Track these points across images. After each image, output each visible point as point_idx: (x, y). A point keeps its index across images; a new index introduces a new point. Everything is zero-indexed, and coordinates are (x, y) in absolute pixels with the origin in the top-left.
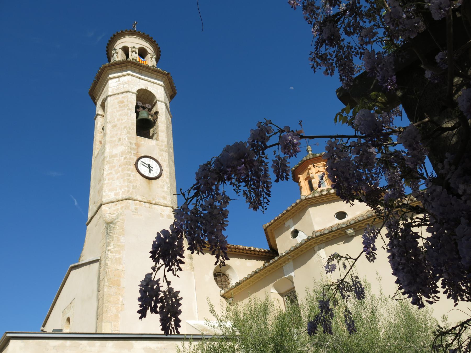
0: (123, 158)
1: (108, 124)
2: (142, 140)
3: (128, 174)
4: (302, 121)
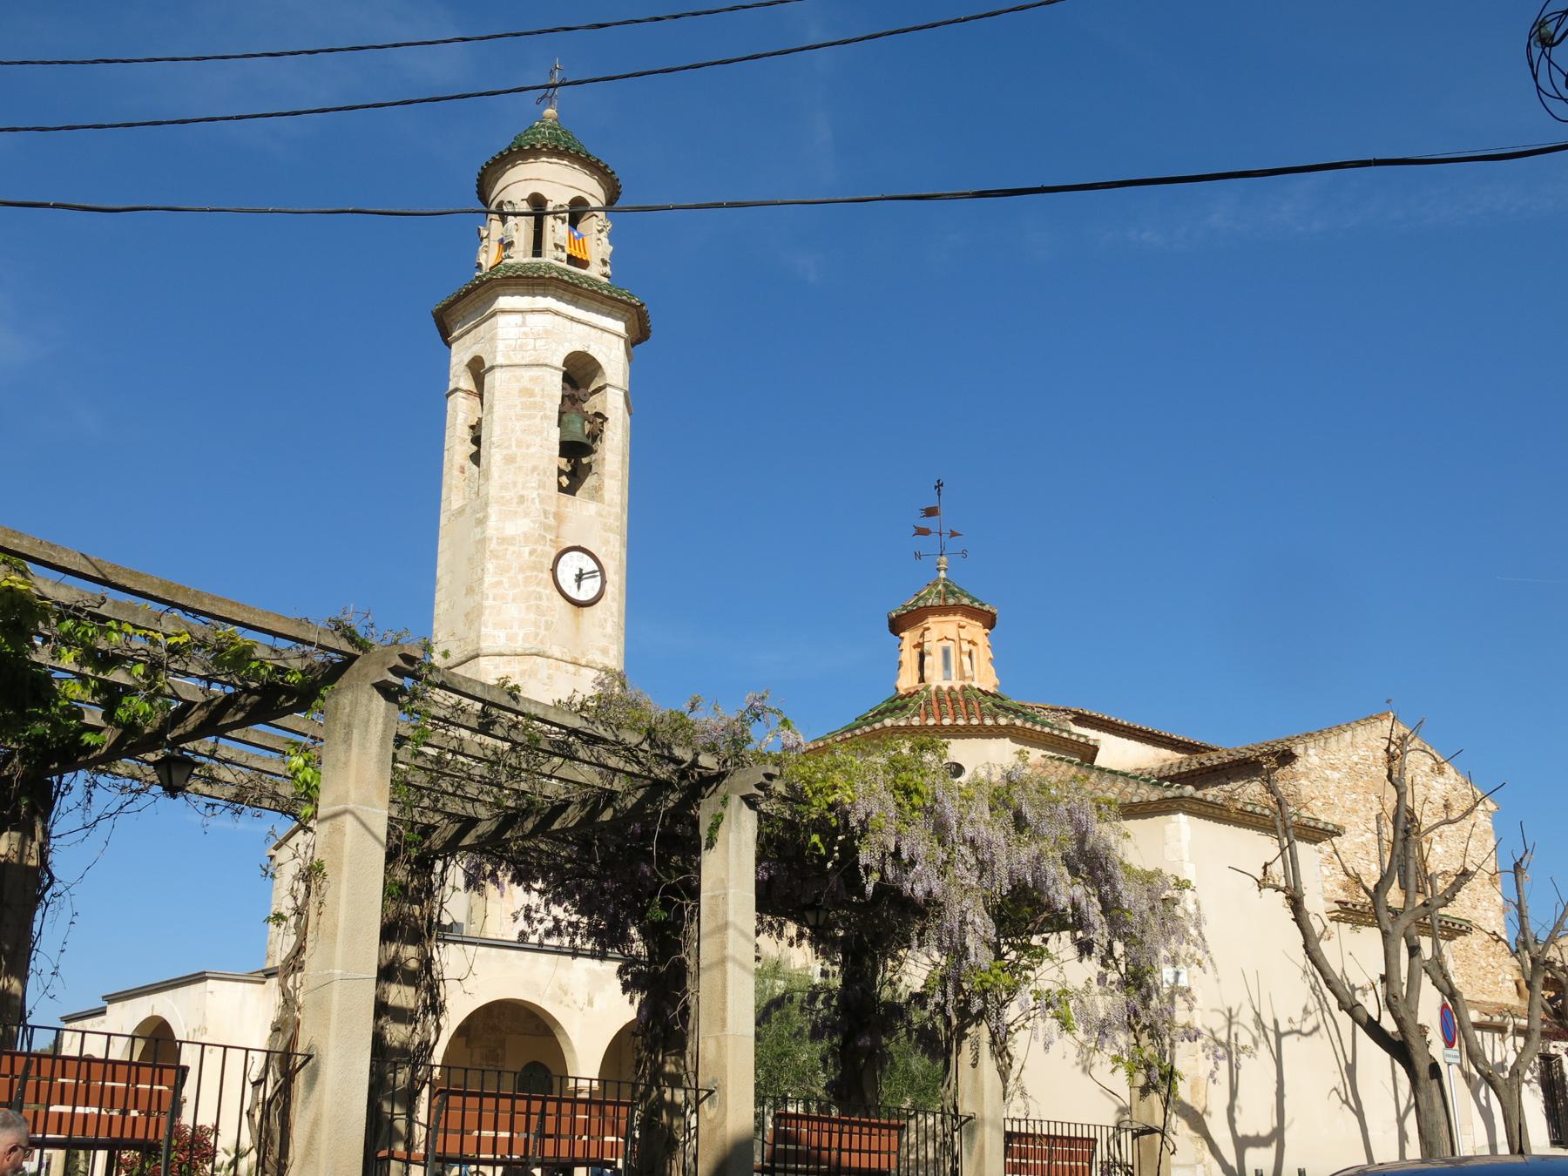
0: (527, 550)
3: (539, 593)
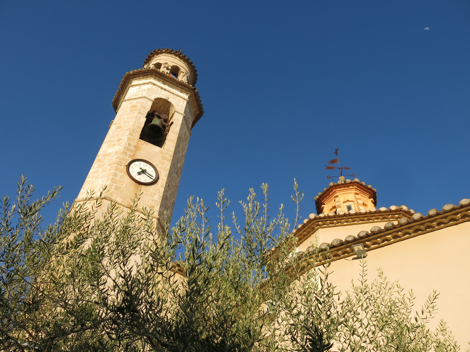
0: (115, 157)
1: (114, 125)
2: (144, 144)
4: (338, 150)
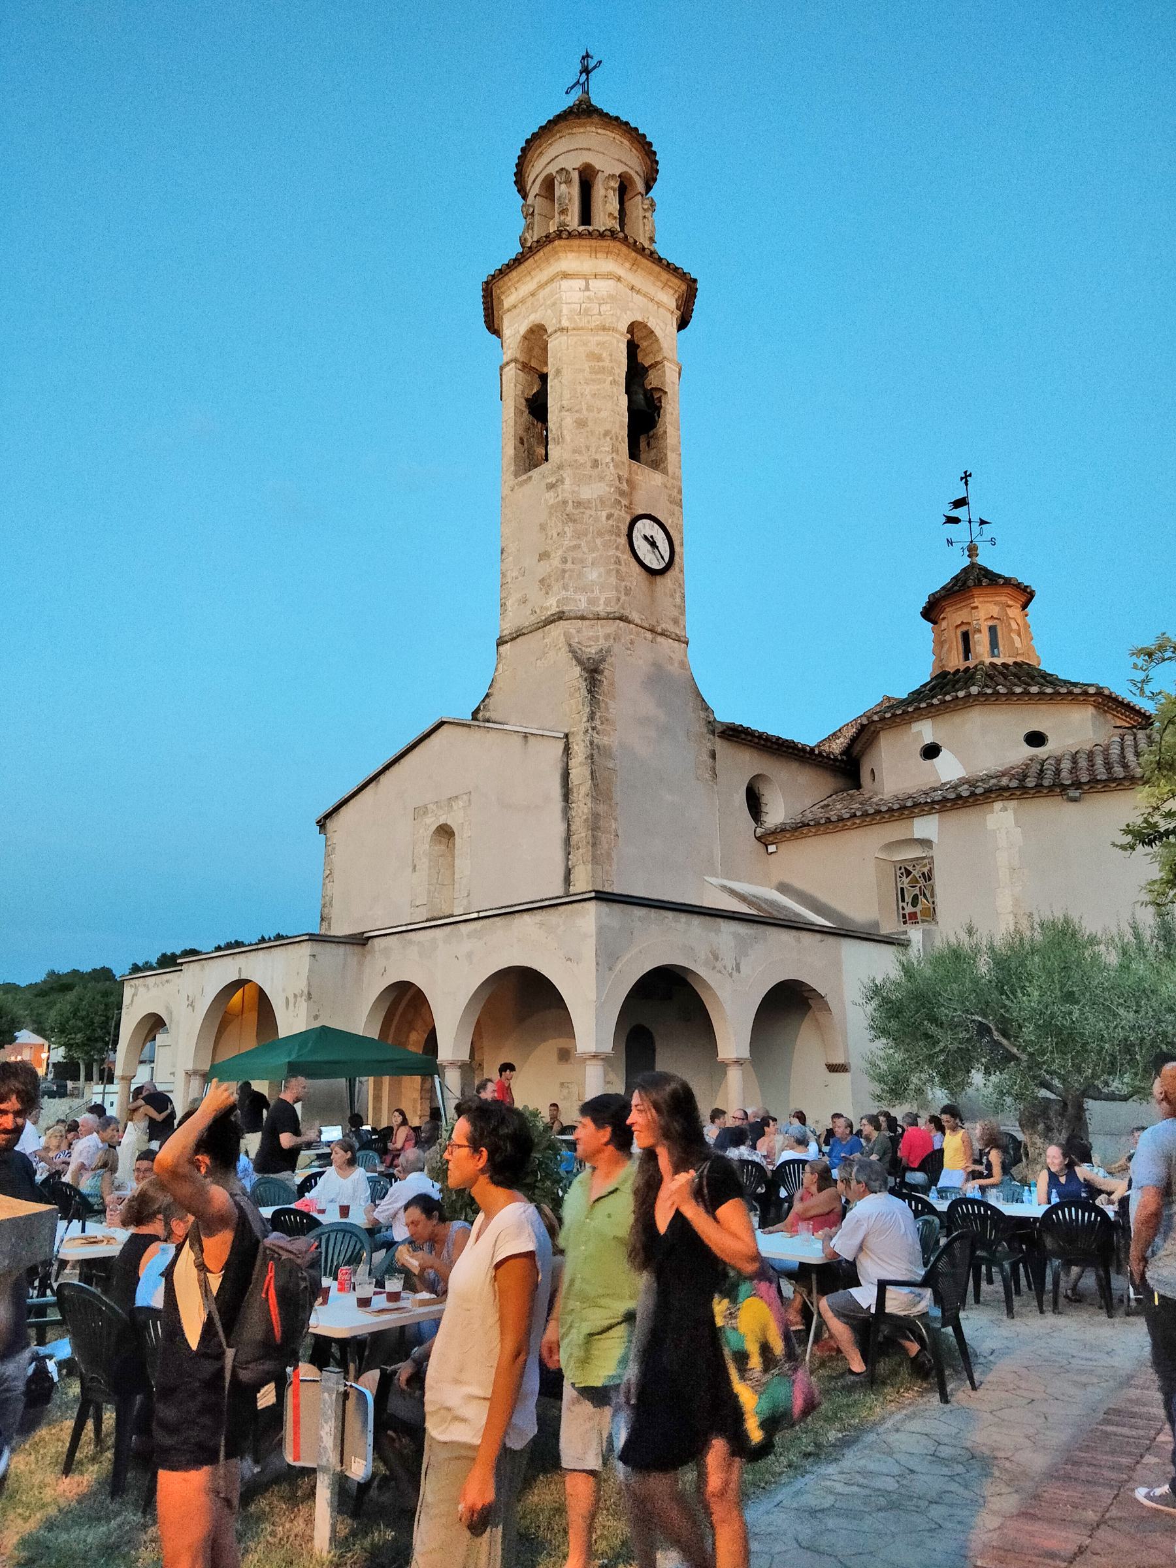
0: (604, 514)
